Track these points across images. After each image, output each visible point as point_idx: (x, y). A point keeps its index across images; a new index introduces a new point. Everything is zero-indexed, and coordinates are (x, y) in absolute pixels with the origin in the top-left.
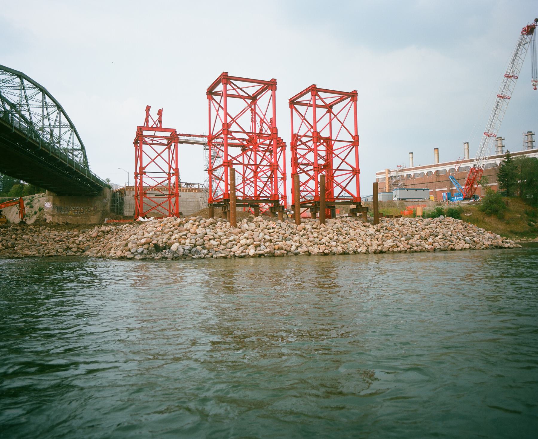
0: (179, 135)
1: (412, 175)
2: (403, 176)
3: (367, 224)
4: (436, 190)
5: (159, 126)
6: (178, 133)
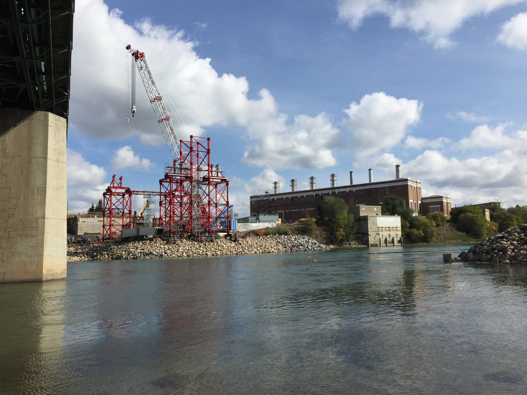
0: (132, 191)
1: (276, 199)
2: (269, 200)
3: (231, 242)
4: (292, 211)
5: (120, 185)
6: (131, 190)
